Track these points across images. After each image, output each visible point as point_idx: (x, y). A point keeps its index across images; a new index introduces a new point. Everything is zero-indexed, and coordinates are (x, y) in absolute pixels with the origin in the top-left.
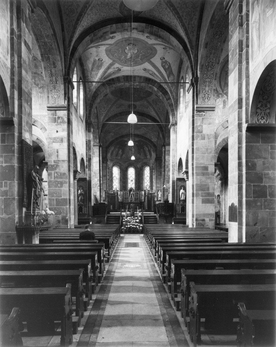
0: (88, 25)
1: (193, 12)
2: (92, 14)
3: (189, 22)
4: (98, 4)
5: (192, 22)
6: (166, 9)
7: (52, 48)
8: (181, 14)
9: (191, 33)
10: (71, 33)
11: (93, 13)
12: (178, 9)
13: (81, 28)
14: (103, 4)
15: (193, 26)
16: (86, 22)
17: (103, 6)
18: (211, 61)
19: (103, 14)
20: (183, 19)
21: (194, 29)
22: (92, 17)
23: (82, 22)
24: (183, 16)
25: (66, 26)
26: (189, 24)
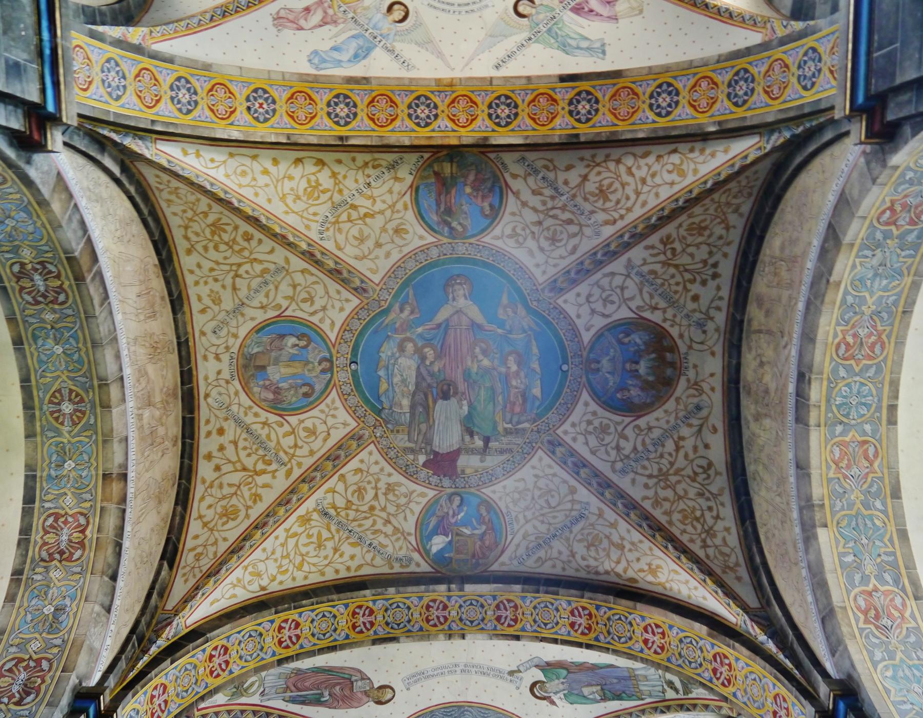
0: (280, 578)
1: (710, 509)
2: (303, 540)
3: (704, 541)
4: (335, 508)
5: (718, 541)
6: (600, 515)
7: (82, 544)
8: (663, 519)
9: (724, 572)
10: (199, 576)
11: (309, 536)
12: (647, 505)
13: (248, 578)
14: (354, 507)
15: (726, 550)
16: (276, 560)
17: (350, 518)
18: (876, 590)
19: (347, 549)
20: (676, 532)
21: (733, 559)
22: (304, 550)
23: (258, 554)
24: (670, 523)
25: (187, 558)
26: (705, 546)
